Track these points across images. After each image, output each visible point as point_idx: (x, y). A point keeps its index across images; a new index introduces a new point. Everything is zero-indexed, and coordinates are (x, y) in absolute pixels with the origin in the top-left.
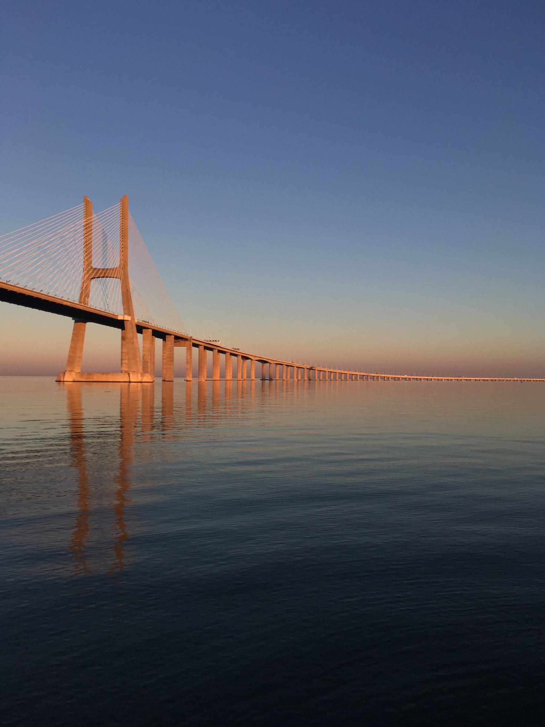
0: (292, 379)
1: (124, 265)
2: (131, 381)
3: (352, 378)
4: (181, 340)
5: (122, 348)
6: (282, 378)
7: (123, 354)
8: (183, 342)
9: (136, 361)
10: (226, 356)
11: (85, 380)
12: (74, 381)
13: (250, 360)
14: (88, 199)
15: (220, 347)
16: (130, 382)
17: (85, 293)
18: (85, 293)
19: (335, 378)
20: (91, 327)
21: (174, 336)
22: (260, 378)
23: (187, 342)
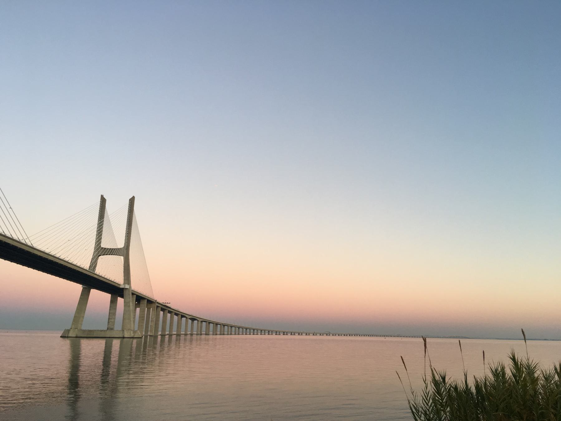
2: (126, 336)
5: (110, 309)
7: (110, 315)
9: (131, 320)
10: (171, 315)
11: (86, 336)
13: (185, 318)
15: (170, 308)
16: (124, 338)
20: (94, 292)
21: (146, 300)
23: (153, 305)
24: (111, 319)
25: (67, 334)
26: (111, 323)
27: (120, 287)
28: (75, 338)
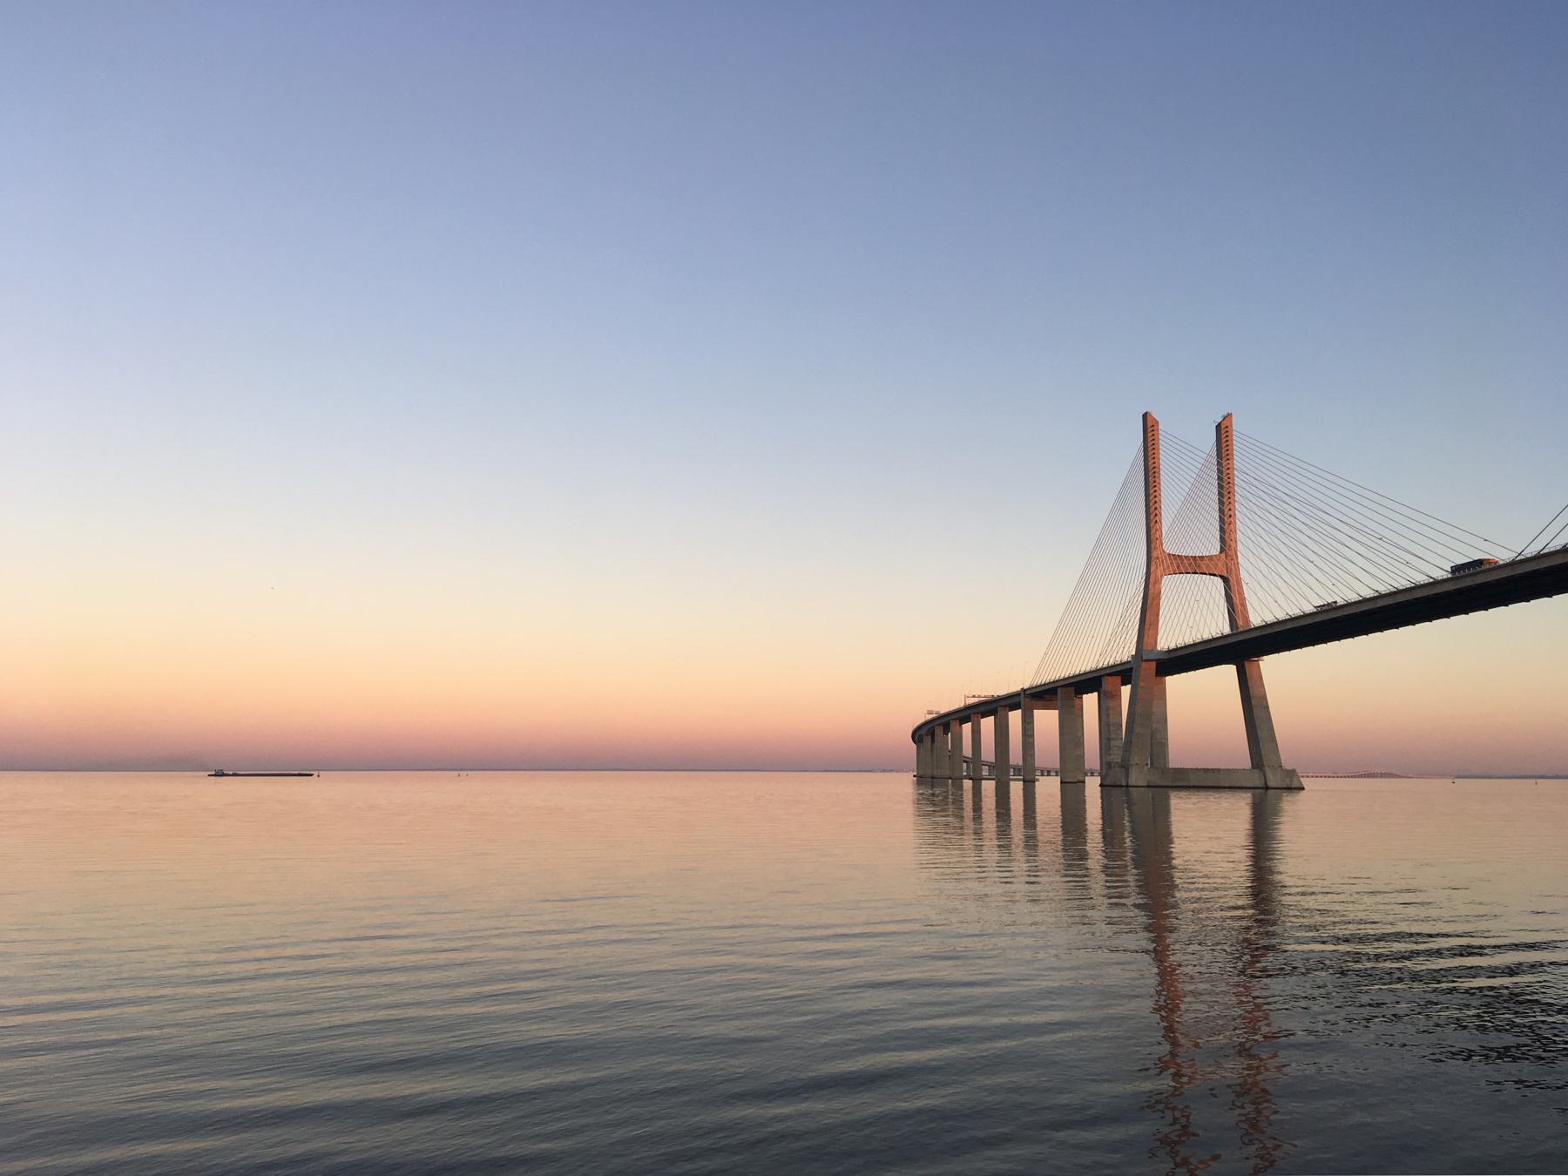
7: (1111, 728)
11: (1171, 784)
12: (1148, 787)
16: (1267, 788)
22: (913, 771)
24: (1114, 739)
25: (1123, 780)
26: (1115, 748)
28: (1146, 789)
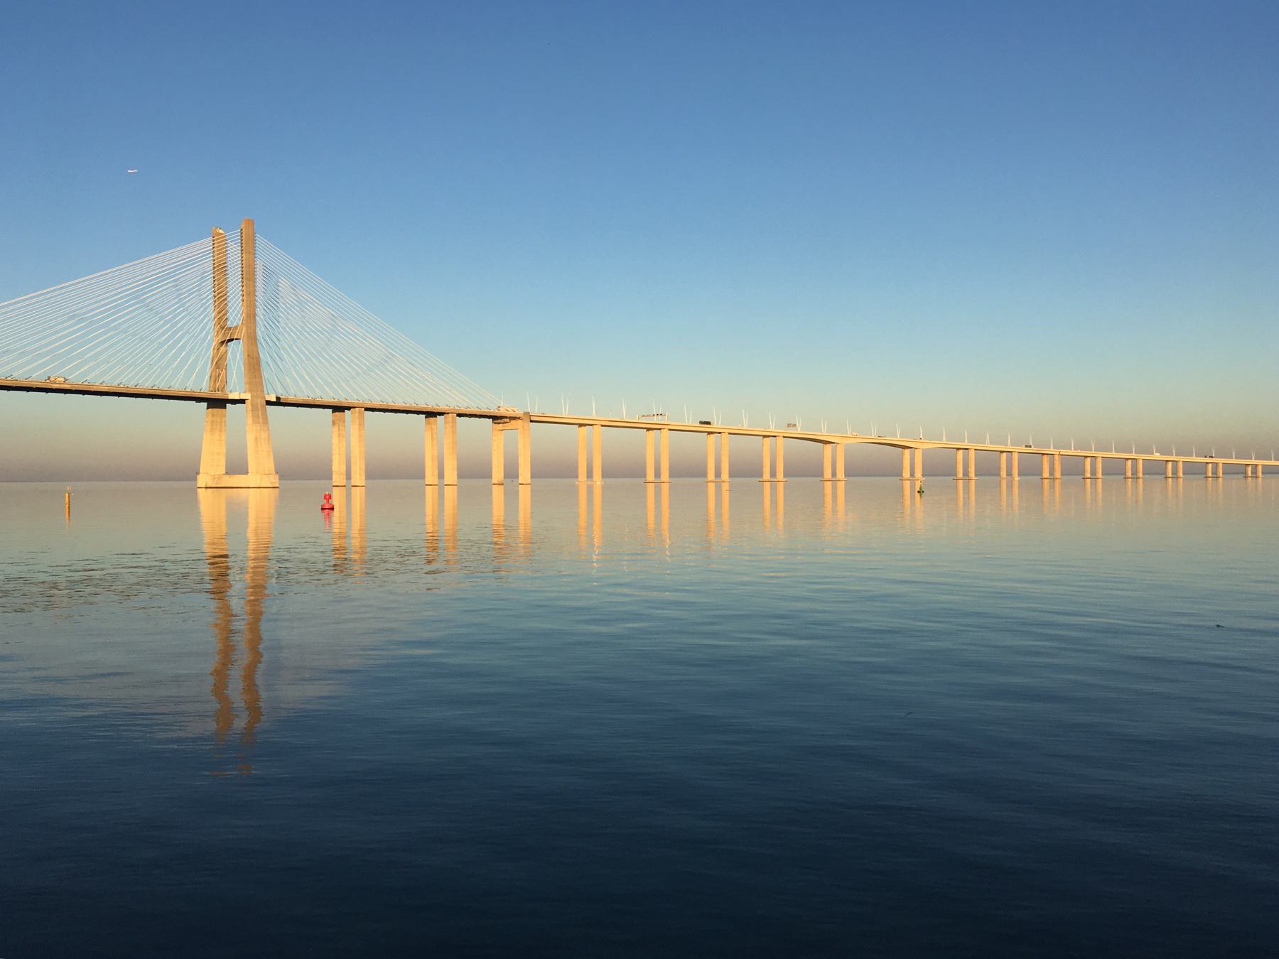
0: (1010, 477)
1: (251, 317)
3: (1246, 473)
4: (508, 420)
6: (968, 475)
8: (513, 422)
12: (206, 488)
14: (221, 231)
17: (220, 364)
18: (220, 364)
19: (1175, 471)
23: (519, 422)
27: (230, 398)
